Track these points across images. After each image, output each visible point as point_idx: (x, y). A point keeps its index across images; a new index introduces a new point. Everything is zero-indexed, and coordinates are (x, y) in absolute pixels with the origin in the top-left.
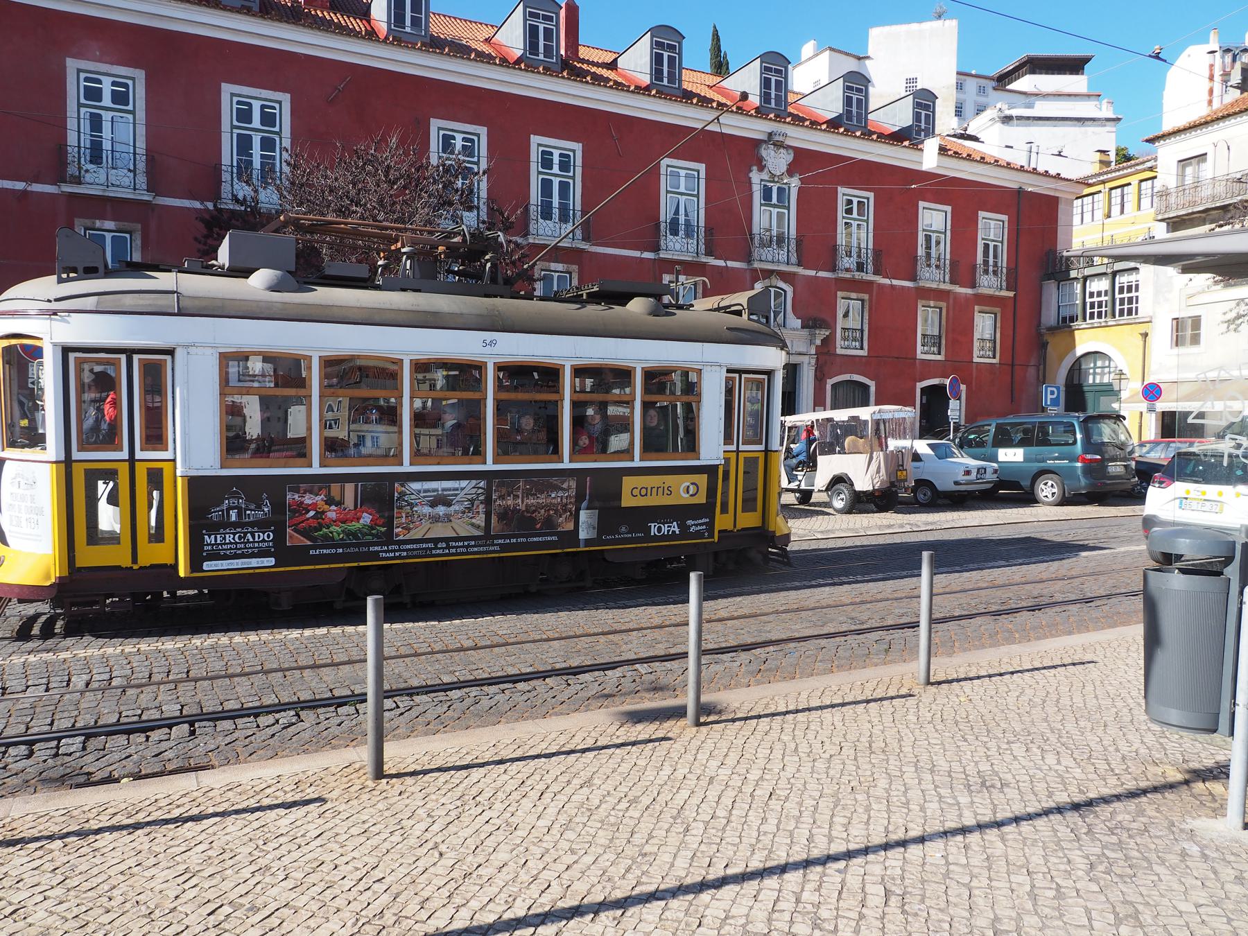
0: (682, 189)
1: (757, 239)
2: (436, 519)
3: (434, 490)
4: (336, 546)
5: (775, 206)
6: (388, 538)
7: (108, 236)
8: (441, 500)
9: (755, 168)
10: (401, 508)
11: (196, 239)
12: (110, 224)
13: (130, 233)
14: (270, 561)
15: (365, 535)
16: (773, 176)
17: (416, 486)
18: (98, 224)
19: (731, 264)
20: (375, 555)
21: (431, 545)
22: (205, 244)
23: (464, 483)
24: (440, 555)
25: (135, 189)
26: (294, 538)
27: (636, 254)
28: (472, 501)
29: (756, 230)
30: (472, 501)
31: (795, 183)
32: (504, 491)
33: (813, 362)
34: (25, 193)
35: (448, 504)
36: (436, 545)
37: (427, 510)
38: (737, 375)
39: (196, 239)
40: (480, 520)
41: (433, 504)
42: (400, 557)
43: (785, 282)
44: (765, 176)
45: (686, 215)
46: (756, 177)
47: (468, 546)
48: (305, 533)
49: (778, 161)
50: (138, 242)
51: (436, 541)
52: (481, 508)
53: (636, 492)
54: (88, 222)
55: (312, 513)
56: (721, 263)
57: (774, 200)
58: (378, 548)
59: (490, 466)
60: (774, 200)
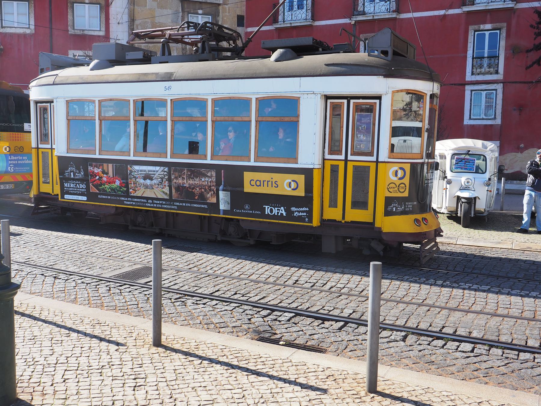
2: (147, 187)
3: (145, 171)
4: (108, 195)
6: (127, 194)
7: (487, 33)
8: (148, 177)
10: (131, 179)
11: (532, 26)
12: (488, 26)
13: (500, 29)
14: (85, 198)
15: (118, 191)
17: (136, 167)
18: (482, 27)
20: (122, 202)
21: (145, 201)
22: (538, 28)
23: (158, 168)
24: (149, 207)
25: (284, 22)
26: (93, 190)
28: (162, 179)
30: (162, 179)
32: (177, 174)
34: (445, 16)
35: (151, 179)
36: (147, 201)
37: (142, 181)
38: (345, 101)
39: (532, 26)
40: (167, 190)
41: (145, 178)
42: (132, 205)
47: (162, 204)
48: (96, 187)
50: (504, 34)
51: (147, 198)
52: (167, 183)
53: (253, 183)
54: (476, 27)
55: (98, 177)
58: (123, 199)
59: (169, 160)
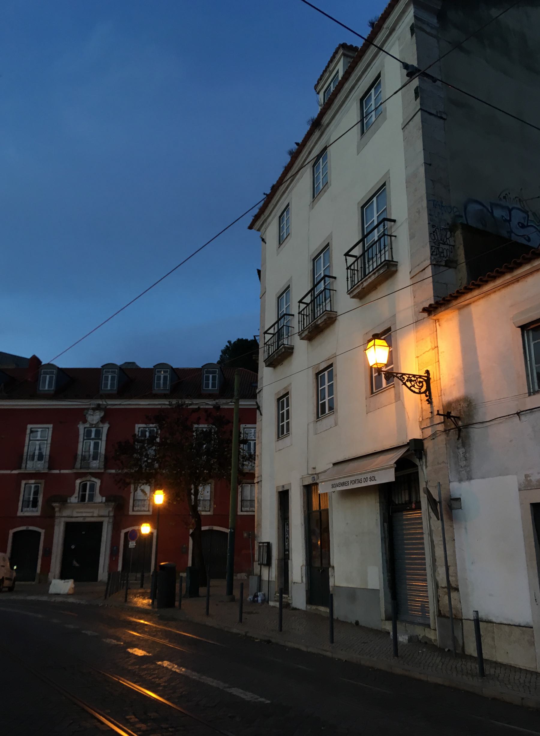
0: (39, 438)
1: (79, 457)
5: (93, 439)
9: (80, 422)
16: (91, 425)
19: (63, 471)
27: (8, 472)
29: (79, 452)
31: (105, 427)
33: (111, 520)
43: (96, 477)
44: (87, 425)
45: (40, 449)
46: (81, 428)
49: (94, 418)
56: (57, 472)
57: (93, 436)
60: (93, 436)
